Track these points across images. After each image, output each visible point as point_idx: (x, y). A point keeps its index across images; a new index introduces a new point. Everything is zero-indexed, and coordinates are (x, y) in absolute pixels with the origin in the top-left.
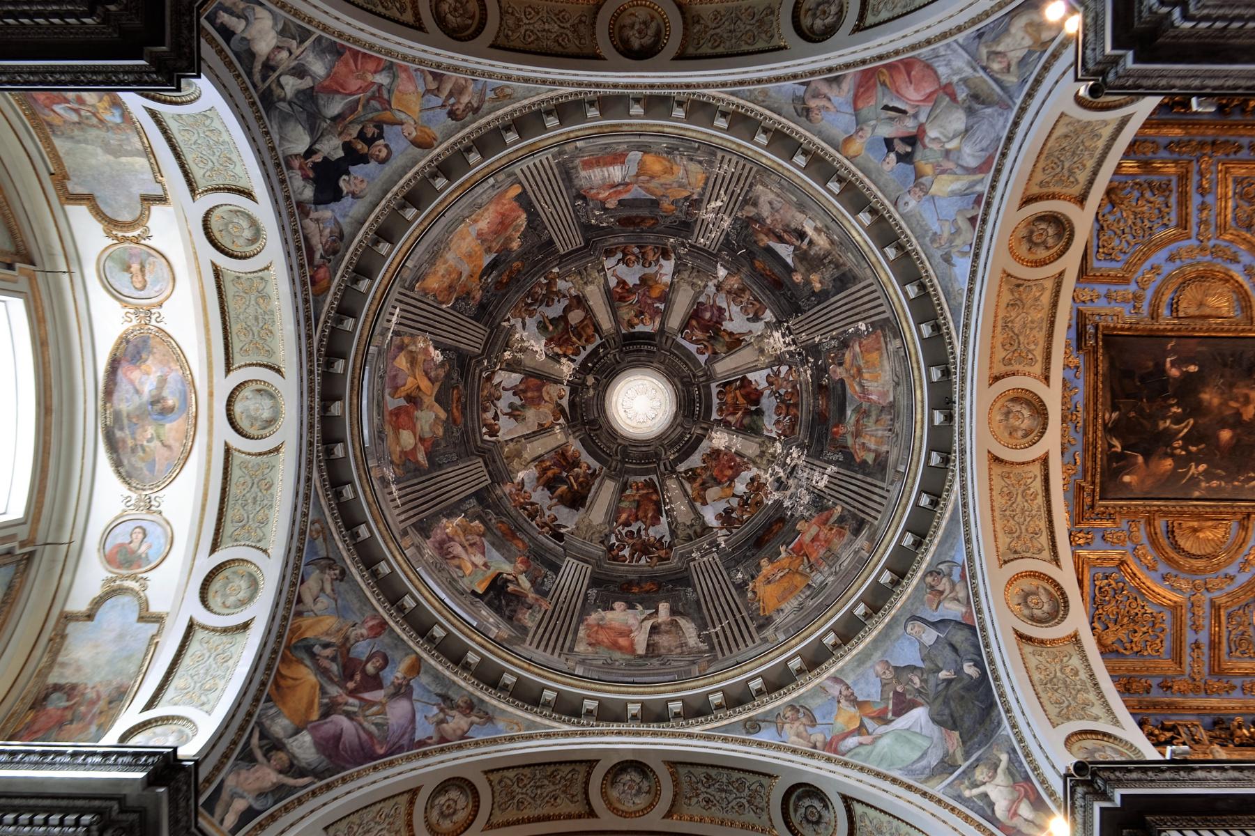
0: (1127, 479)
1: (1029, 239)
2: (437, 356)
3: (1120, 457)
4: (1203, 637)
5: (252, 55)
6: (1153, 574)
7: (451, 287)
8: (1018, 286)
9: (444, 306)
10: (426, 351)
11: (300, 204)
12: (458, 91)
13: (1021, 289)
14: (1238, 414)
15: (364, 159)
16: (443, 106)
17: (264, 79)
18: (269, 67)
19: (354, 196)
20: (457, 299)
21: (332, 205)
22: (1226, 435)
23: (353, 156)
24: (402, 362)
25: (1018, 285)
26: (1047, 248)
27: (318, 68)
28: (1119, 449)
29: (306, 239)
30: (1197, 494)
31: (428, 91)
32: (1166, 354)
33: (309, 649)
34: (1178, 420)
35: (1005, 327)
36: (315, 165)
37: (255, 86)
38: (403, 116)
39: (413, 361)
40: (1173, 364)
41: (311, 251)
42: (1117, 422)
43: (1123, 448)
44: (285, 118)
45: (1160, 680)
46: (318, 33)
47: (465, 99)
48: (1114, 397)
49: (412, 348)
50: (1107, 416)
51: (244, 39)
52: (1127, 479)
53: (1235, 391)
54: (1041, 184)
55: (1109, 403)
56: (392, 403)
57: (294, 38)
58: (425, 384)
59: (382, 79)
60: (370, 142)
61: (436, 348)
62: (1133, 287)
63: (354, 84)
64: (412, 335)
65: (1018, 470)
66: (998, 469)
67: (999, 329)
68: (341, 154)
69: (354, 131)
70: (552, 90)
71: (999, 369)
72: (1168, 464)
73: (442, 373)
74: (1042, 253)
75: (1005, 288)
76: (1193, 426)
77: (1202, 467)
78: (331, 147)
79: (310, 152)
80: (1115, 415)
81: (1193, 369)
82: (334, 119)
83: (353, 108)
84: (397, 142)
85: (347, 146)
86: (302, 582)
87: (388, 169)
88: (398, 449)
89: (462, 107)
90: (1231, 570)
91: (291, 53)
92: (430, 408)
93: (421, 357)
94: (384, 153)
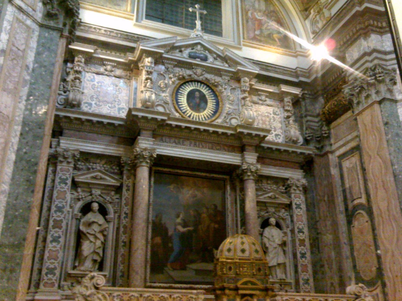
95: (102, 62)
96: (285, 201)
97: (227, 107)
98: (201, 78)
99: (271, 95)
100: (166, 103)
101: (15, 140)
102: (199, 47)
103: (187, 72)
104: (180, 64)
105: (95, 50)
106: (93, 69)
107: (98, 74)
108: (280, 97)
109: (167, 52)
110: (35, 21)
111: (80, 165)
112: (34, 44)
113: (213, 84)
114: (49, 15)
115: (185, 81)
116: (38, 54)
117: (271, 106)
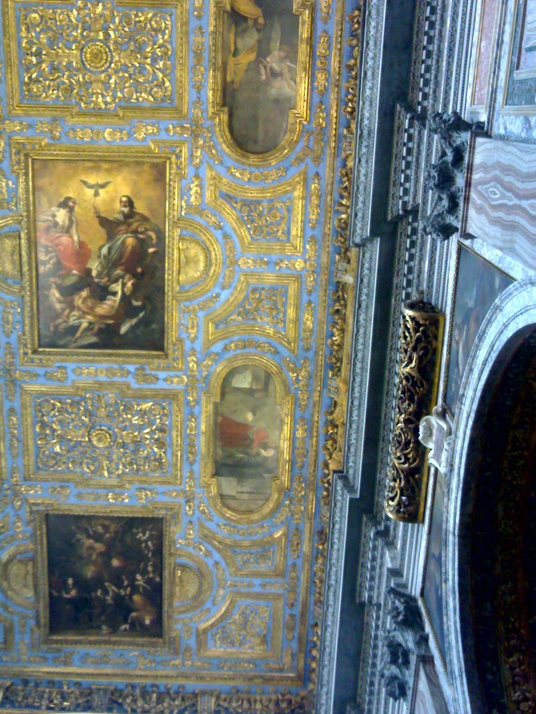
0: (147, 622)
3: (133, 626)
4: (257, 581)
6: (213, 610)
14: (101, 554)
22: (115, 563)
28: (127, 626)
30: (158, 579)
32: (60, 598)
34: (106, 592)
40: (68, 592)
42: (109, 626)
43: (126, 622)
45: (287, 608)
48: (92, 627)
50: (105, 632)
52: (147, 622)
53: (85, 555)
55: (95, 631)
62: (16, 619)
72: (136, 598)
76: (111, 581)
77: (139, 577)
80: (104, 627)
81: (70, 581)
90: (210, 562)
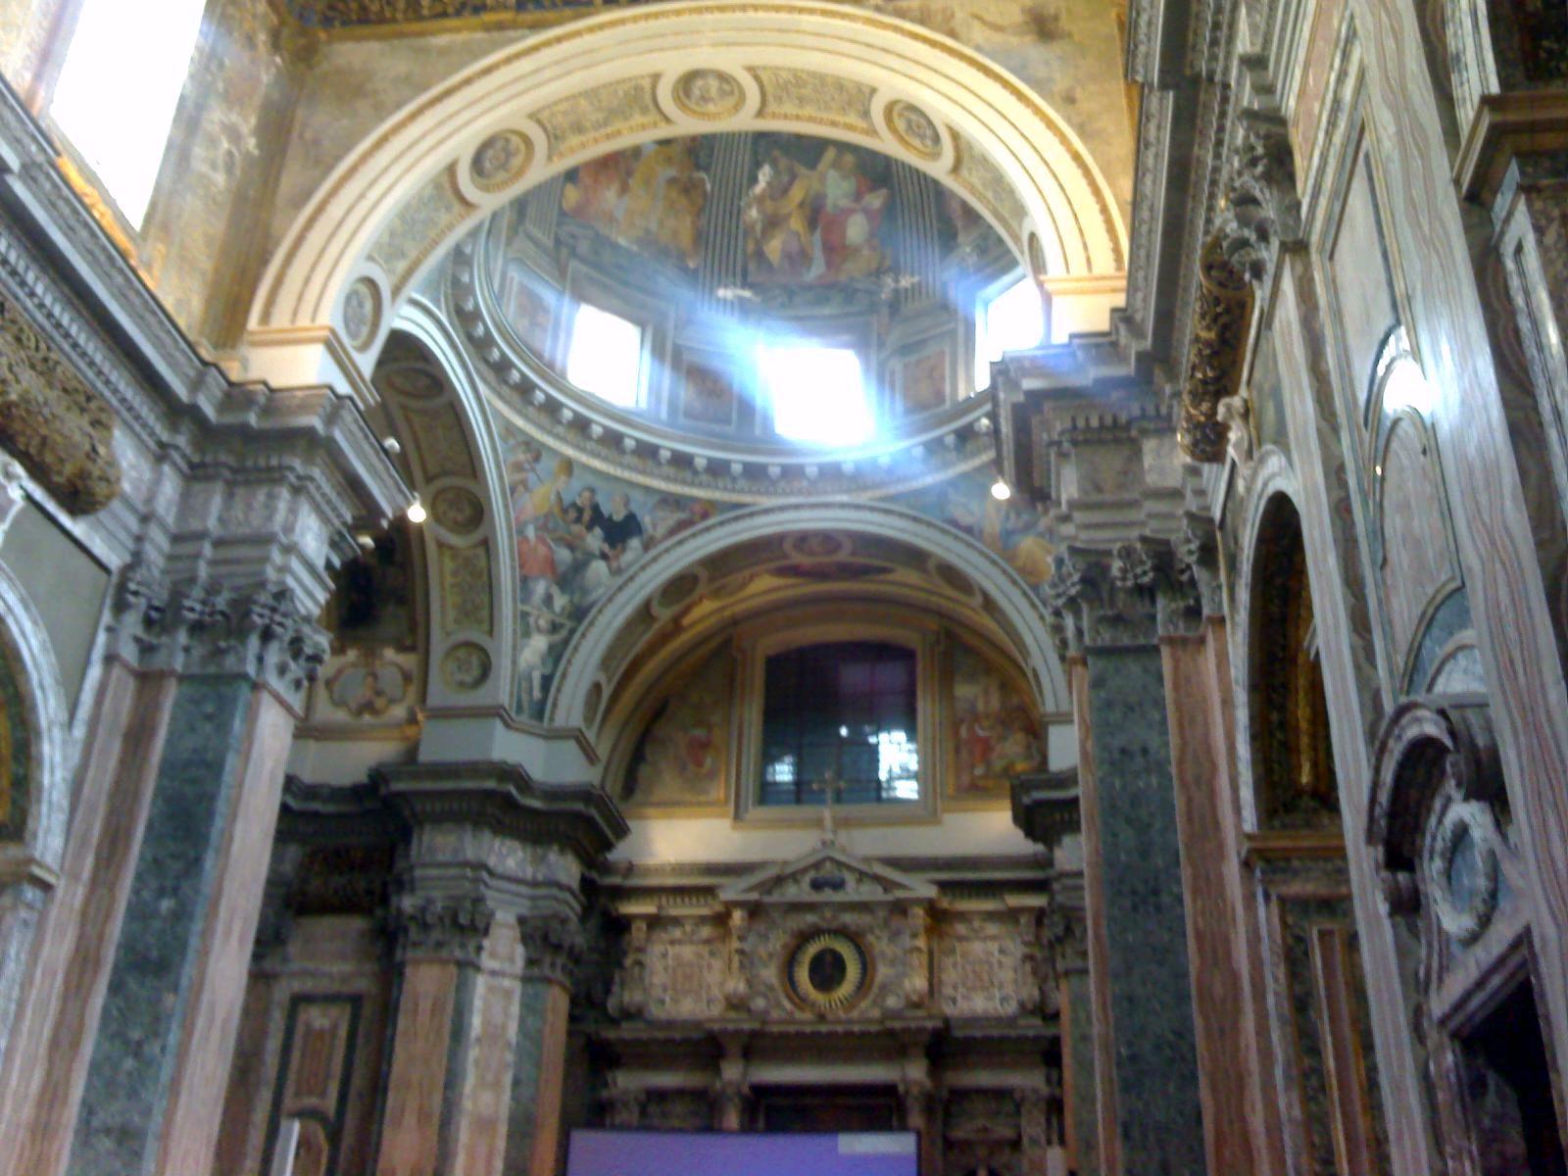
1: (504, 166)
2: (765, 175)
5: (551, 647)
7: (688, 188)
8: (556, 137)
9: (708, 187)
10: (760, 200)
11: (646, 547)
12: (518, 467)
13: (559, 133)
15: (596, 508)
16: (533, 470)
17: (562, 626)
18: (554, 628)
19: (627, 503)
20: (698, 167)
21: (639, 518)
23: (598, 518)
24: (774, 247)
25: (554, 137)
26: (507, 141)
27: (540, 588)
29: (672, 532)
31: (527, 489)
33: (1009, 534)
35: (606, 123)
36: (612, 545)
37: (572, 632)
38: (553, 497)
39: (773, 223)
41: (682, 525)
44: (585, 591)
46: (520, 607)
47: (521, 457)
49: (758, 228)
51: (544, 663)
54: (448, 209)
56: (817, 269)
57: (528, 625)
58: (797, 193)
59: (531, 532)
60: (580, 511)
61: (753, 180)
63: (542, 550)
64: (745, 236)
65: (769, 89)
66: (772, 107)
67: (609, 130)
68: (598, 531)
69: (577, 528)
70: (489, 403)
71: (653, 116)
73: (783, 162)
74: (515, 140)
75: (563, 147)
78: (595, 540)
79: (604, 556)
82: (572, 548)
83: (560, 541)
84: (573, 490)
85: (590, 527)
86: (955, 523)
87: (598, 484)
88: (865, 252)
89: (529, 456)
91: (539, 617)
92: (823, 179)
93: (769, 206)
94: (587, 494)
95: (676, 921)
96: (1009, 1133)
97: (883, 972)
98: (834, 925)
99: (991, 916)
100: (771, 988)
101: (501, 1144)
102: (828, 864)
103: (811, 918)
104: (797, 907)
105: (660, 907)
106: (664, 936)
107: (672, 942)
108: (1012, 915)
109: (769, 892)
110: (513, 976)
111: (653, 1109)
112: (515, 1009)
113: (857, 934)
114: (530, 962)
115: (805, 937)
116: (522, 1021)
117: (993, 938)
